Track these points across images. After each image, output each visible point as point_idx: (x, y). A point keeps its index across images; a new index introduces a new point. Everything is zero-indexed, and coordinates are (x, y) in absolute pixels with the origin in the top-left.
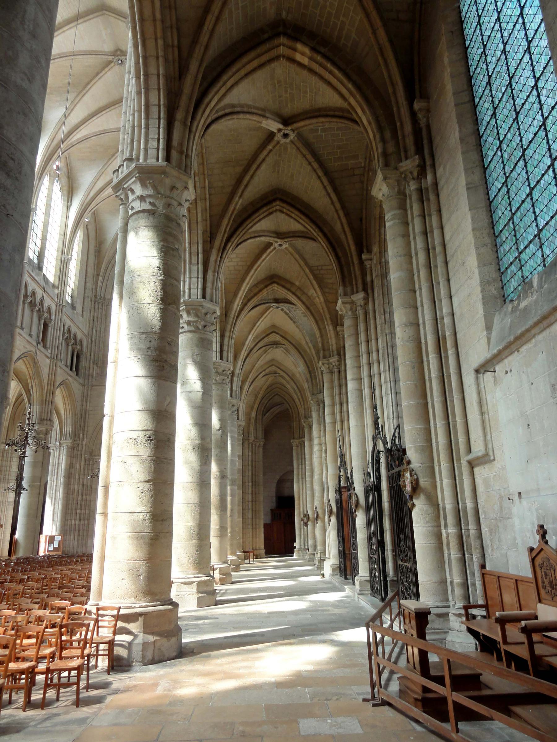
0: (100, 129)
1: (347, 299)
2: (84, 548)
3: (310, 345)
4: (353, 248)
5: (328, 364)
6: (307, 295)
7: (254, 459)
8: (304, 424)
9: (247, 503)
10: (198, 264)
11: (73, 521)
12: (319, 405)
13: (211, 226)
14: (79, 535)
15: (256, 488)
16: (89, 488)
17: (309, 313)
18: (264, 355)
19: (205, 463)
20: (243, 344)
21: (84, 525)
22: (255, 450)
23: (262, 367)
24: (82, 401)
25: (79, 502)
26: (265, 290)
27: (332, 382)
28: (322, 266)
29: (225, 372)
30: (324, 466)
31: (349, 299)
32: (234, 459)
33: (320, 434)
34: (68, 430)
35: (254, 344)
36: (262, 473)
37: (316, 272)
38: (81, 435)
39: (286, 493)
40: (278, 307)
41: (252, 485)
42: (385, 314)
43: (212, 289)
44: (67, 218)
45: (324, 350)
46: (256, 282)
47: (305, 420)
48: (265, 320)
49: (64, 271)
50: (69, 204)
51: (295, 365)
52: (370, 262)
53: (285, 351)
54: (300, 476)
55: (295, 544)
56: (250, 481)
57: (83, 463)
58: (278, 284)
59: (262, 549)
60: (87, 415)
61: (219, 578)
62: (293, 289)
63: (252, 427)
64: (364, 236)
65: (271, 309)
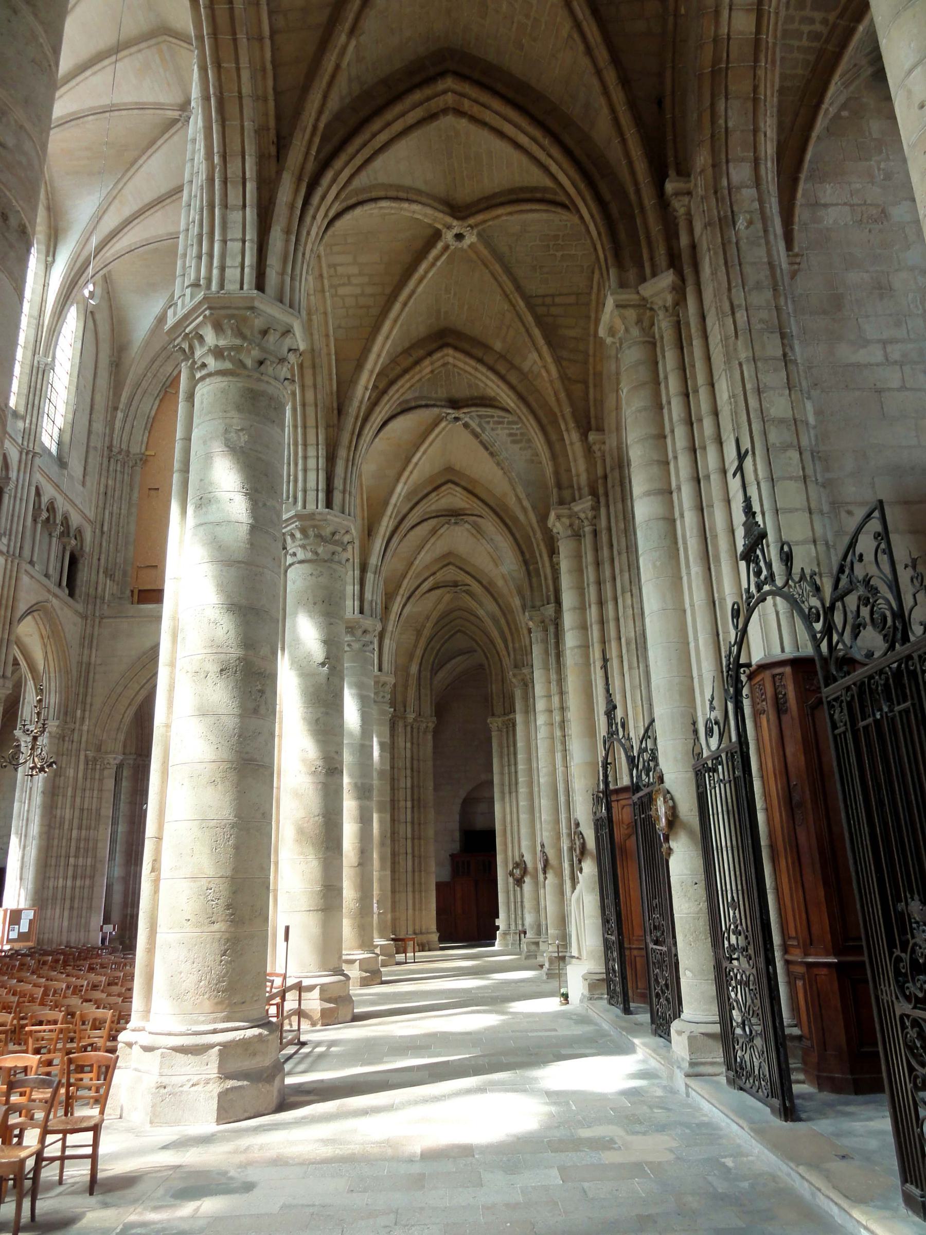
0: (105, 101)
1: (628, 296)
2: (82, 933)
3: (526, 503)
4: (641, 167)
5: (570, 517)
6: (519, 370)
7: (415, 757)
8: (514, 680)
10: (244, 206)
11: (61, 880)
12: (546, 630)
13: (278, 118)
14: (72, 908)
16: (93, 817)
17: (525, 410)
18: (432, 540)
19: (256, 711)
20: (386, 503)
21: (82, 888)
23: (427, 567)
24: (82, 645)
25: (73, 844)
26: (427, 362)
27: (578, 556)
28: (553, 296)
29: (337, 537)
30: (559, 756)
31: (636, 297)
32: (367, 743)
33: (549, 689)
34: (52, 701)
36: (430, 785)
37: (541, 310)
38: (79, 712)
39: (480, 824)
40: (457, 419)
41: (413, 807)
42: (733, 313)
43: (283, 273)
44: (45, 286)
45: (559, 486)
46: (407, 345)
47: (516, 671)
48: (429, 451)
49: (39, 386)
50: (50, 259)
51: (494, 561)
52: (686, 199)
53: (474, 532)
54: (507, 789)
55: (498, 922)
56: (409, 798)
57: (81, 767)
58: (456, 348)
60: (91, 675)
61: (319, 1008)
62: (489, 359)
63: (412, 693)
64: (670, 137)
65: (443, 424)
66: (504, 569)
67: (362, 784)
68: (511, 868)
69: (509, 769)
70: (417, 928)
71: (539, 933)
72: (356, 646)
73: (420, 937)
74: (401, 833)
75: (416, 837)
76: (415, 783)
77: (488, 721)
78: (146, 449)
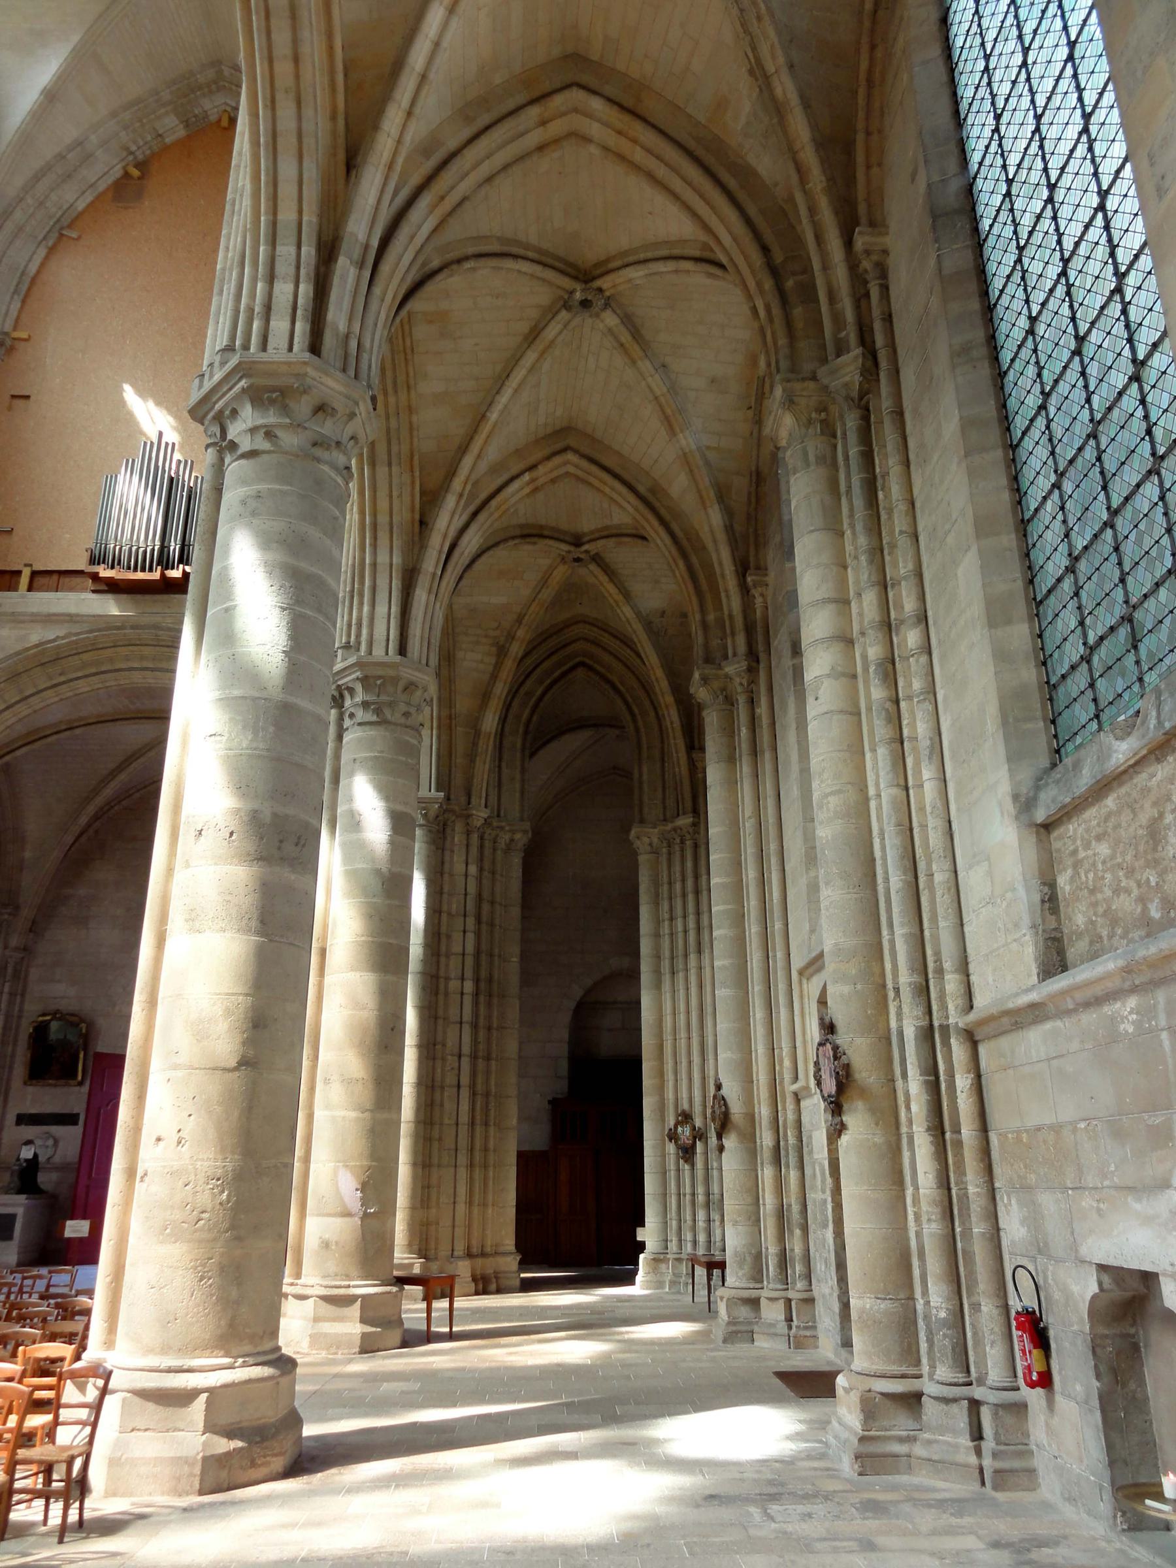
3: (786, 88)
7: (486, 894)
9: (452, 1061)
12: (829, 431)
15: (489, 1005)
18: (531, 357)
22: (493, 862)
30: (878, 763)
35: (467, 133)
39: (607, 1044)
41: (476, 994)
47: (709, 670)
51: (667, 419)
53: (626, 337)
54: (666, 965)
55: (642, 1235)
56: (469, 973)
59: (504, 1254)
63: (483, 768)
66: (687, 441)
67: (275, 815)
68: (672, 1123)
69: (671, 926)
70: (475, 1243)
71: (757, 1275)
72: (290, 440)
73: (479, 1261)
74: (449, 1044)
75: (482, 1056)
76: (484, 947)
77: (633, 833)
78: (15, 328)
